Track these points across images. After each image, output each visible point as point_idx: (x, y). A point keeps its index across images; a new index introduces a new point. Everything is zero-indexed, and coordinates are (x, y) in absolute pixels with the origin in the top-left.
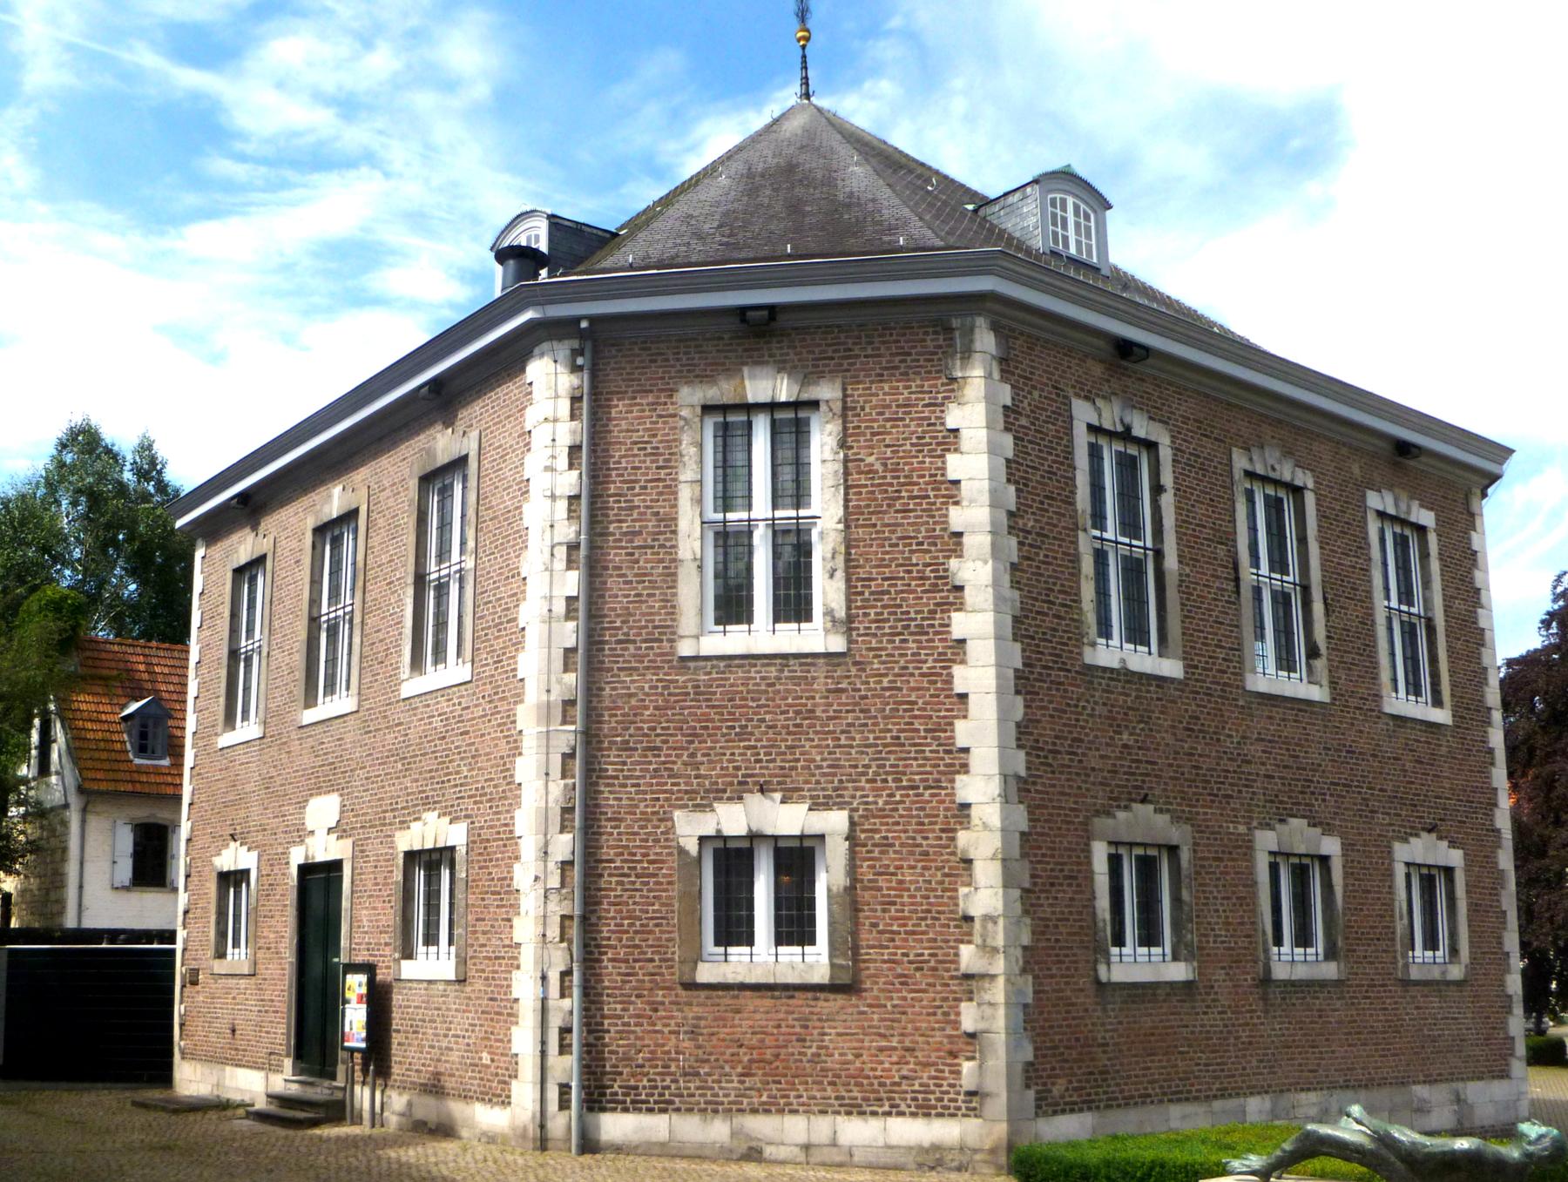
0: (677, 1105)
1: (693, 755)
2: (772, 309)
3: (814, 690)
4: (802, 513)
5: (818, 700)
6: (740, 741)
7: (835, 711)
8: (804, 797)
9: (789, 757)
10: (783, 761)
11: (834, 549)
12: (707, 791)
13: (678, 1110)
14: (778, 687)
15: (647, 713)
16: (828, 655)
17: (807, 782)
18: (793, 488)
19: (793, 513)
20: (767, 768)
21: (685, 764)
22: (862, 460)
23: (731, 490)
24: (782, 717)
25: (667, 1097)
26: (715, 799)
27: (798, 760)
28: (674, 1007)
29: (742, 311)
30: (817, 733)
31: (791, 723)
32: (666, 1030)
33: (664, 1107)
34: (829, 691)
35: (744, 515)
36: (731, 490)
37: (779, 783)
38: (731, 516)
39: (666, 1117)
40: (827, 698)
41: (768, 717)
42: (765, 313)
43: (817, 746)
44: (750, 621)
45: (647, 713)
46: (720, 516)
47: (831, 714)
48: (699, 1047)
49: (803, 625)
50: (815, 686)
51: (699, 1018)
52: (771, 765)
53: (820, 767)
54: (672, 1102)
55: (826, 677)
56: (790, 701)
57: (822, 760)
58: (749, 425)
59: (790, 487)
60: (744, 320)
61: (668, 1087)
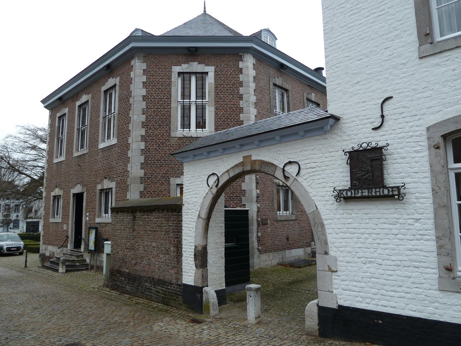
2: (197, 48)
4: (203, 101)
18: (201, 94)
19: (201, 101)
23: (185, 94)
29: (189, 48)
35: (189, 101)
36: (185, 94)
38: (184, 101)
42: (195, 49)
44: (190, 128)
46: (182, 101)
49: (204, 129)
58: (190, 78)
59: (201, 94)
60: (189, 51)
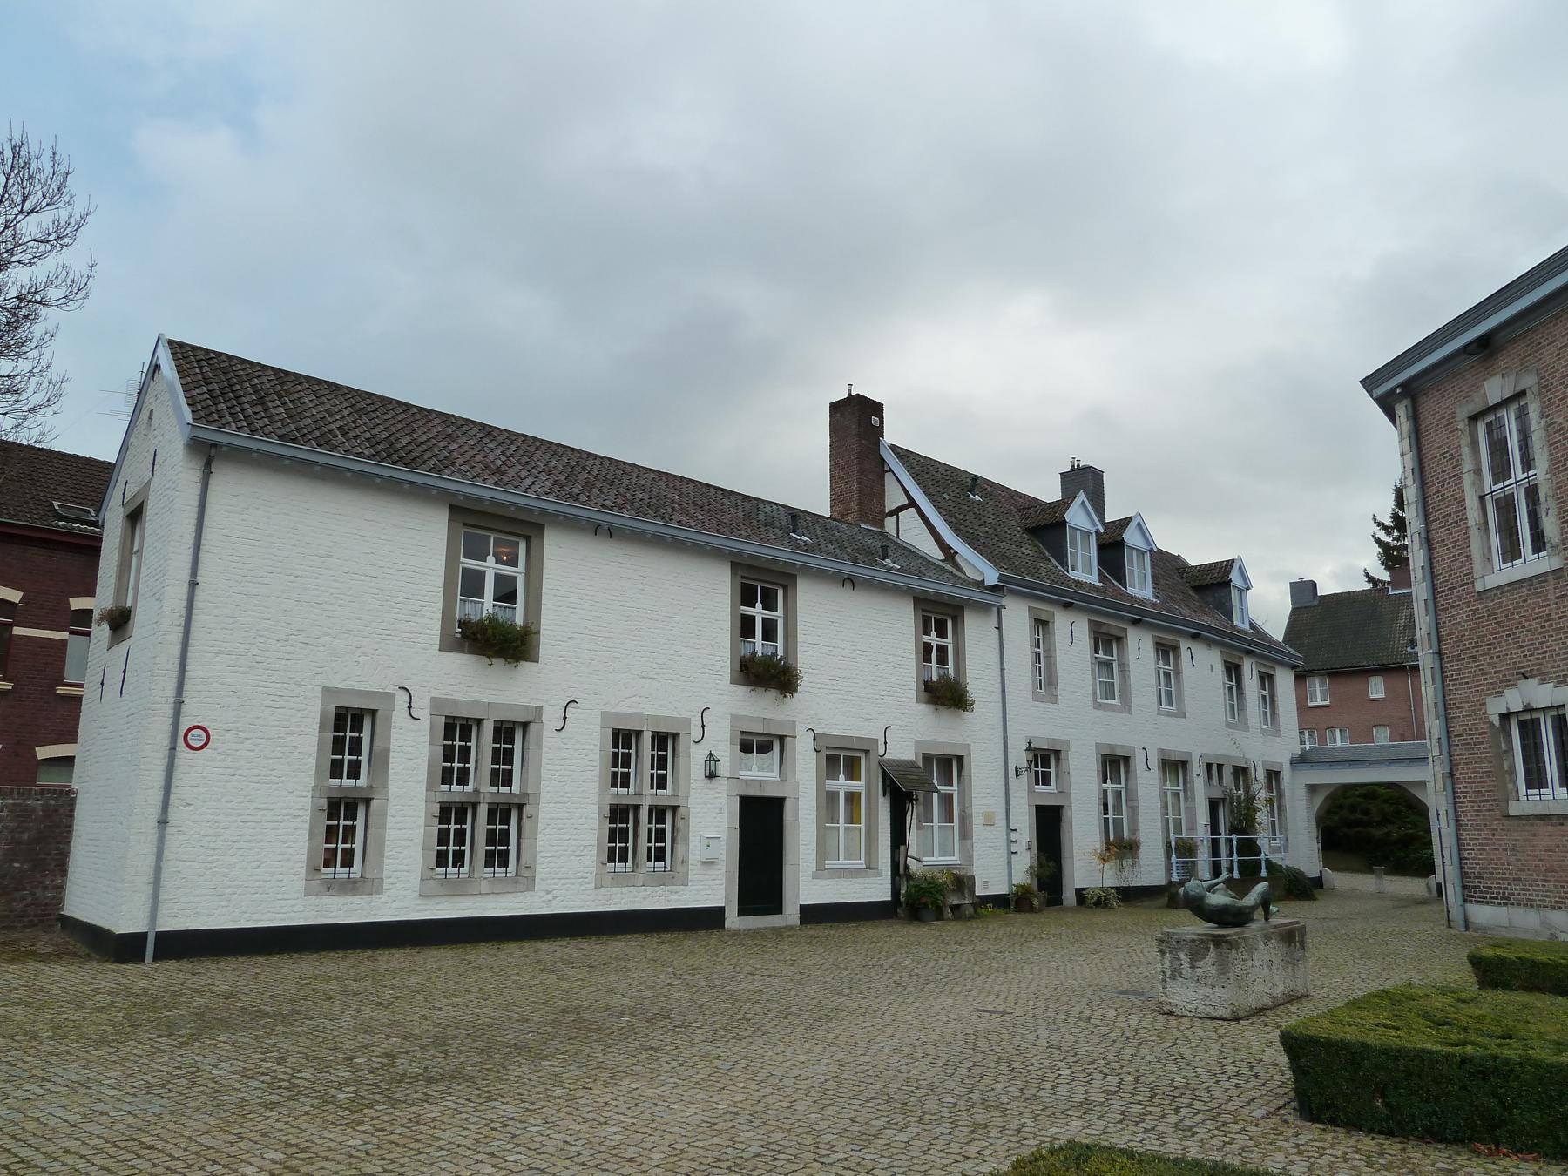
0: (1512, 901)
1: (1492, 658)
3: (1548, 600)
5: (1552, 606)
6: (1515, 643)
7: (1562, 612)
8: (1551, 678)
9: (1541, 651)
10: (1539, 654)
11: (1546, 494)
12: (1501, 682)
13: (1512, 904)
14: (1529, 601)
15: (1467, 634)
16: (1553, 572)
17: (1553, 667)
20: (1530, 661)
21: (1489, 664)
22: (1556, 422)
24: (1534, 623)
25: (1506, 895)
26: (1506, 686)
27: (1546, 652)
28: (1503, 833)
30: (1554, 630)
31: (1539, 625)
32: (1501, 848)
33: (1505, 902)
34: (1557, 598)
37: (1538, 670)
39: (1505, 908)
40: (1556, 604)
41: (1527, 624)
43: (1555, 640)
45: (1467, 634)
47: (1560, 615)
48: (1518, 860)
50: (1549, 597)
51: (1516, 840)
52: (1532, 658)
53: (1558, 655)
54: (1508, 899)
55: (1555, 589)
56: (1537, 610)
57: (1560, 649)
61: (1506, 889)
